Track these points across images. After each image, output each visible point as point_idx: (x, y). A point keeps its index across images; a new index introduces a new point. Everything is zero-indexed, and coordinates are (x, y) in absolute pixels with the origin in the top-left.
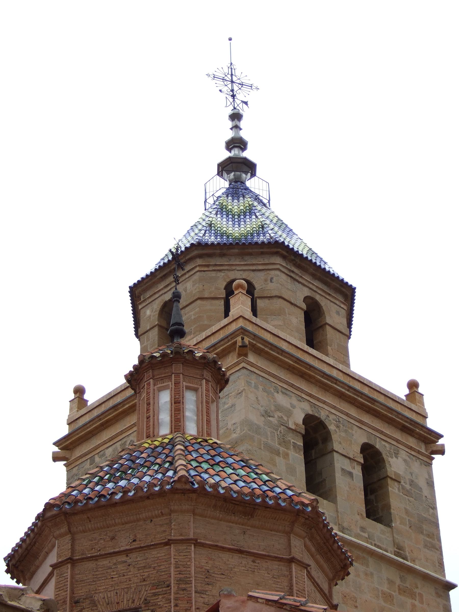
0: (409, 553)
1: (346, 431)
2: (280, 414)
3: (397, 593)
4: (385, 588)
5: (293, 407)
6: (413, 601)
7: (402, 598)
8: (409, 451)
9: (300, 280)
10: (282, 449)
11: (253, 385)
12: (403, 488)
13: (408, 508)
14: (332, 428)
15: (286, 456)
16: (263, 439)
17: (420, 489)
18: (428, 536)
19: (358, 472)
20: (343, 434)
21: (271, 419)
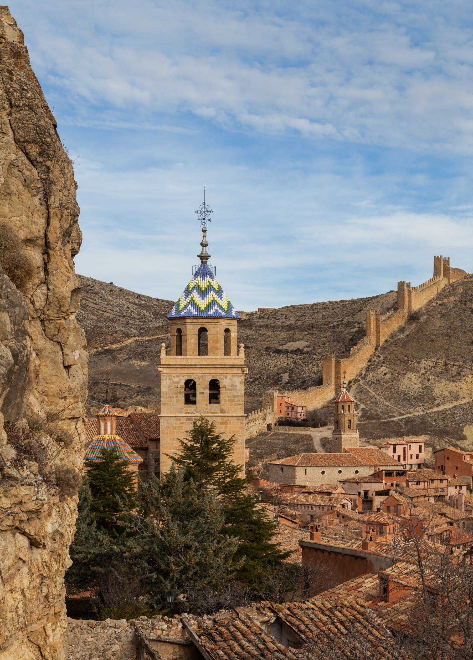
10: (175, 396)
13: (229, 395)
17: (236, 386)
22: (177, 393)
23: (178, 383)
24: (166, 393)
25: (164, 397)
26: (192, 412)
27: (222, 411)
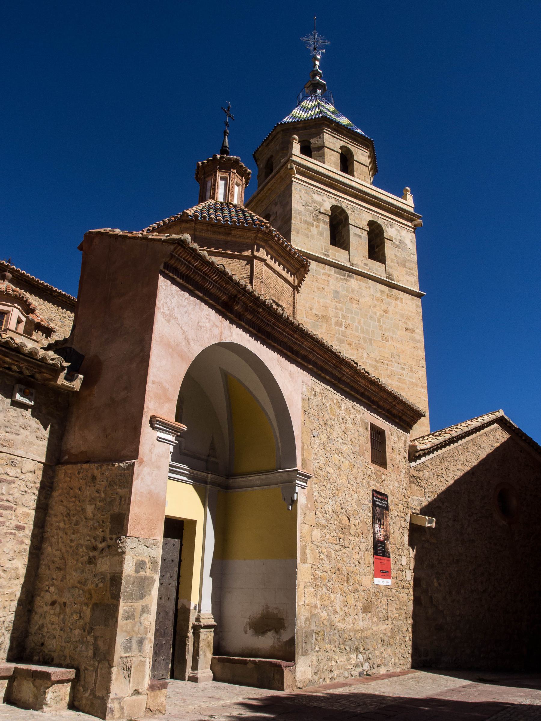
0: (396, 277)
1: (358, 214)
2: (315, 205)
3: (386, 298)
4: (378, 295)
5: (325, 201)
6: (397, 302)
7: (390, 300)
8: (400, 225)
9: (338, 137)
10: (315, 223)
11: (298, 190)
12: (394, 244)
14: (349, 212)
15: (318, 226)
16: (303, 218)
18: (409, 269)
19: (365, 235)
20: (356, 216)
21: (309, 207)
22: (318, 220)
23: (321, 205)
24: (300, 213)
25: (296, 217)
26: (342, 260)
27: (389, 275)
